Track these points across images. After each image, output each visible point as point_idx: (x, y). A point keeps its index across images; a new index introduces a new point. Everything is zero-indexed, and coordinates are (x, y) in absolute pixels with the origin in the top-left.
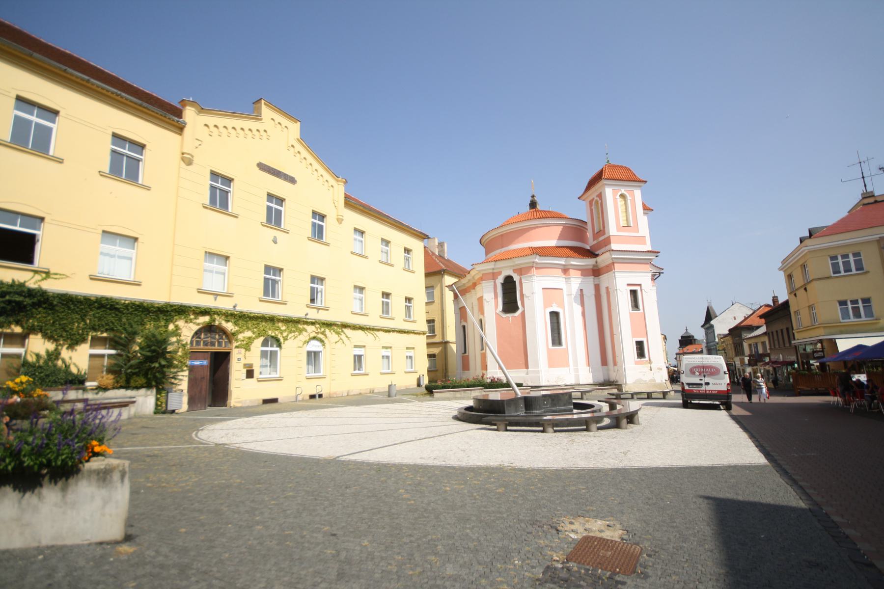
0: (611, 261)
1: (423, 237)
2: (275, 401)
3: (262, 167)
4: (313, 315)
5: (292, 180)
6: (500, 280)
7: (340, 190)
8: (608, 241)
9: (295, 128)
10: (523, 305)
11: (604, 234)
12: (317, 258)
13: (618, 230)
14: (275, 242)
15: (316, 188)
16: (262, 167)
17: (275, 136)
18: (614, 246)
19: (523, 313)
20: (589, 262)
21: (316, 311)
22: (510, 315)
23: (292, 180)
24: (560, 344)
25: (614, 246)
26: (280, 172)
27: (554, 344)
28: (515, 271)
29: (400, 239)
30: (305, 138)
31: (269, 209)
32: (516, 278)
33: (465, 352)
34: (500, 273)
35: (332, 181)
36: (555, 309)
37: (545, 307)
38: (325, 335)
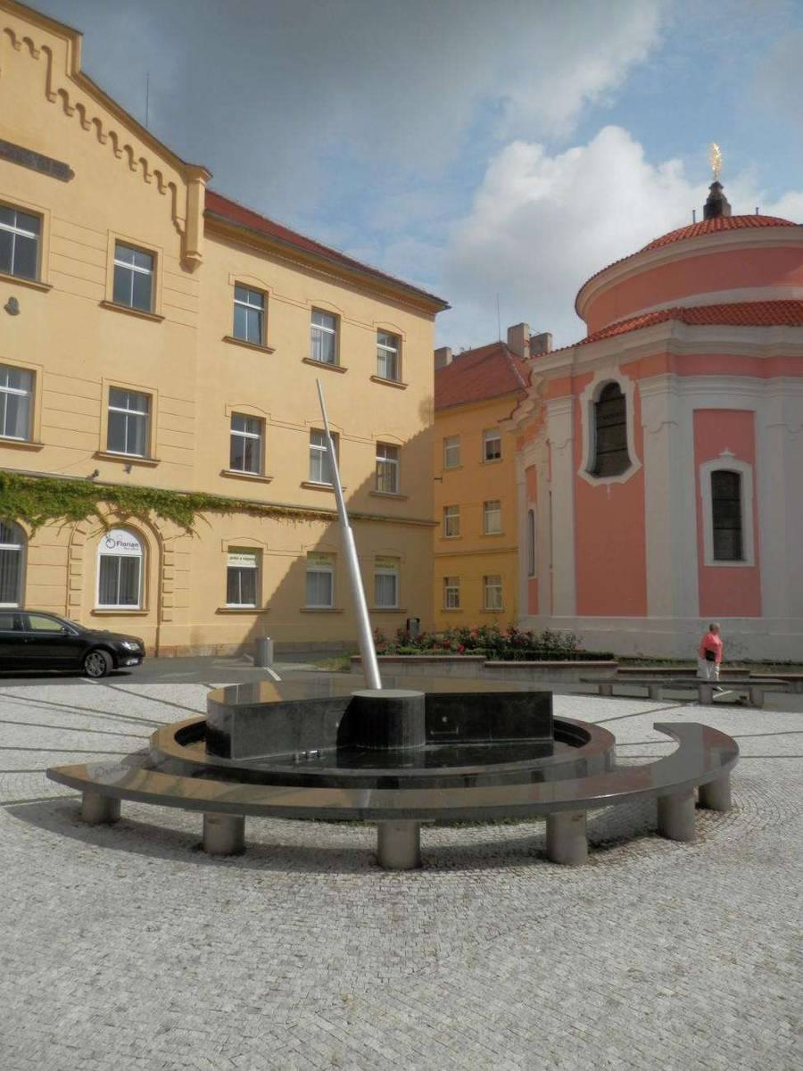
4: (112, 474)
5: (61, 171)
6: (588, 395)
10: (640, 456)
12: (129, 351)
19: (641, 472)
21: (122, 466)
22: (608, 481)
23: (61, 171)
24: (737, 554)
26: (29, 153)
28: (625, 369)
29: (363, 316)
31: (120, 274)
32: (627, 387)
33: (533, 574)
34: (589, 377)
36: (726, 462)
38: (148, 522)
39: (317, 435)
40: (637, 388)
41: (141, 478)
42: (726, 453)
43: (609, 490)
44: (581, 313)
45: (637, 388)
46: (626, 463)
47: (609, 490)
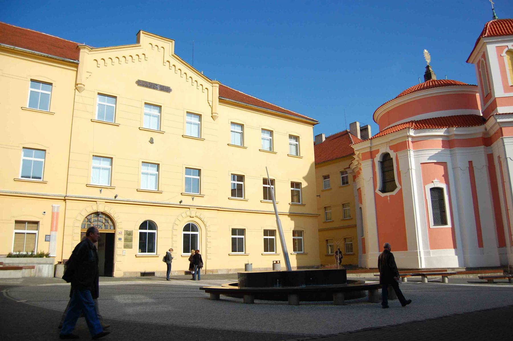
0: (497, 127)
1: (313, 123)
2: (153, 274)
3: (141, 83)
5: (166, 89)
6: (378, 158)
7: (214, 90)
8: (494, 106)
9: (169, 46)
10: (400, 183)
11: (491, 97)
13: (505, 91)
14: (151, 141)
15: (194, 90)
16: (141, 83)
17: (154, 54)
18: (501, 110)
20: (476, 131)
21: (191, 198)
23: (166, 89)
25: (501, 110)
27: (436, 223)
28: (391, 148)
30: (179, 52)
32: (393, 155)
34: (377, 151)
35: (206, 84)
37: (425, 183)
39: (265, 181)
40: (397, 155)
41: (198, 201)
42: (436, 180)
43: (389, 198)
44: (375, 120)
45: (397, 155)
46: (396, 187)
47: (389, 198)
